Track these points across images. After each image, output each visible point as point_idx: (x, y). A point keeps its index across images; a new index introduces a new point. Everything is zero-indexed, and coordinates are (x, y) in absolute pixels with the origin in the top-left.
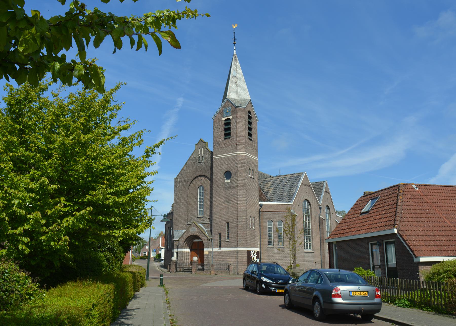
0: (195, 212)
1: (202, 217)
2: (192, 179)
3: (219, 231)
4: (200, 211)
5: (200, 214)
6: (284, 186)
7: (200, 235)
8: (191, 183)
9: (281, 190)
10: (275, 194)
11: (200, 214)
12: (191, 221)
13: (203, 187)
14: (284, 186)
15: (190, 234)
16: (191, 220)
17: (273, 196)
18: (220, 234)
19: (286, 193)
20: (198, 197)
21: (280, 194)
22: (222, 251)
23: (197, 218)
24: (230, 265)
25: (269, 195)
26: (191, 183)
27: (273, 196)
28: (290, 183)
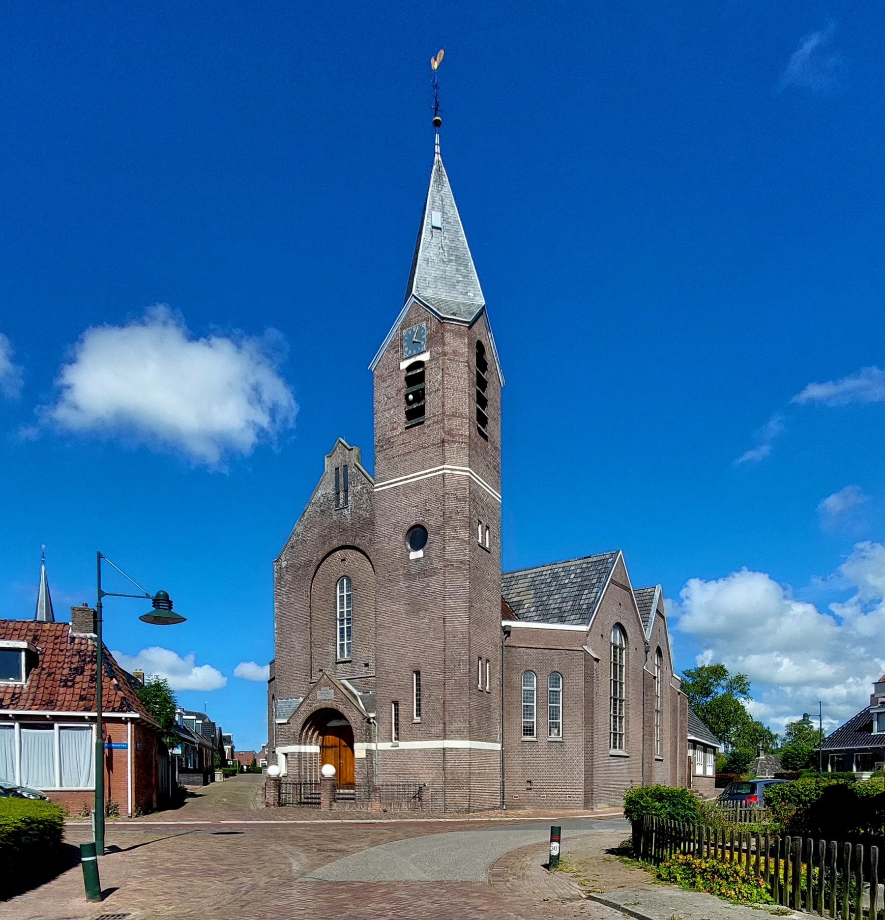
0: (331, 649)
1: (350, 662)
2: (320, 557)
3: (394, 697)
4: (342, 645)
5: (342, 656)
6: (564, 586)
7: (341, 708)
8: (316, 571)
9: (556, 597)
10: (541, 608)
11: (342, 656)
12: (321, 674)
13: (349, 580)
14: (564, 586)
15: (316, 706)
16: (321, 670)
17: (534, 614)
18: (396, 704)
19: (570, 603)
20: (336, 607)
21: (552, 606)
22: (403, 750)
23: (337, 663)
24: (425, 785)
25: (524, 611)
26: (316, 571)
27: (534, 614)
28: (579, 580)
